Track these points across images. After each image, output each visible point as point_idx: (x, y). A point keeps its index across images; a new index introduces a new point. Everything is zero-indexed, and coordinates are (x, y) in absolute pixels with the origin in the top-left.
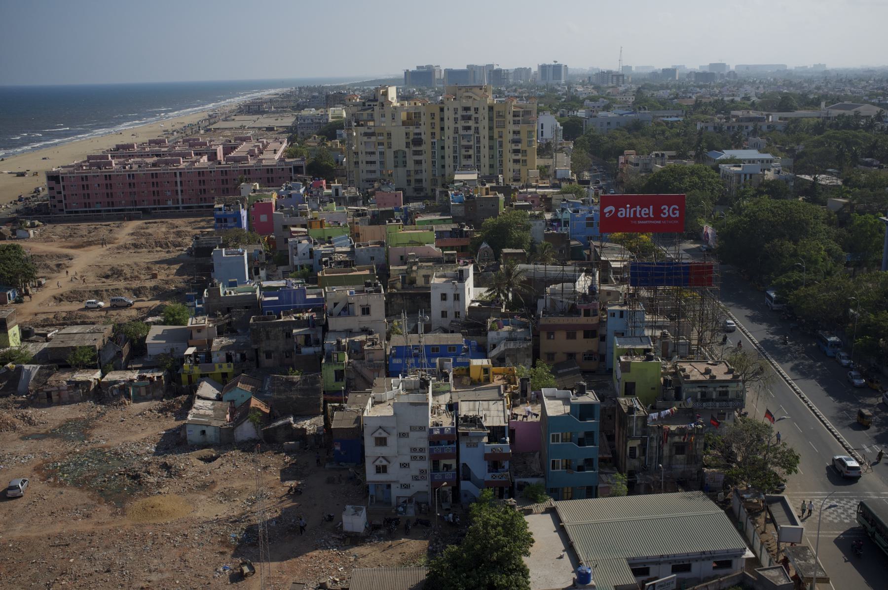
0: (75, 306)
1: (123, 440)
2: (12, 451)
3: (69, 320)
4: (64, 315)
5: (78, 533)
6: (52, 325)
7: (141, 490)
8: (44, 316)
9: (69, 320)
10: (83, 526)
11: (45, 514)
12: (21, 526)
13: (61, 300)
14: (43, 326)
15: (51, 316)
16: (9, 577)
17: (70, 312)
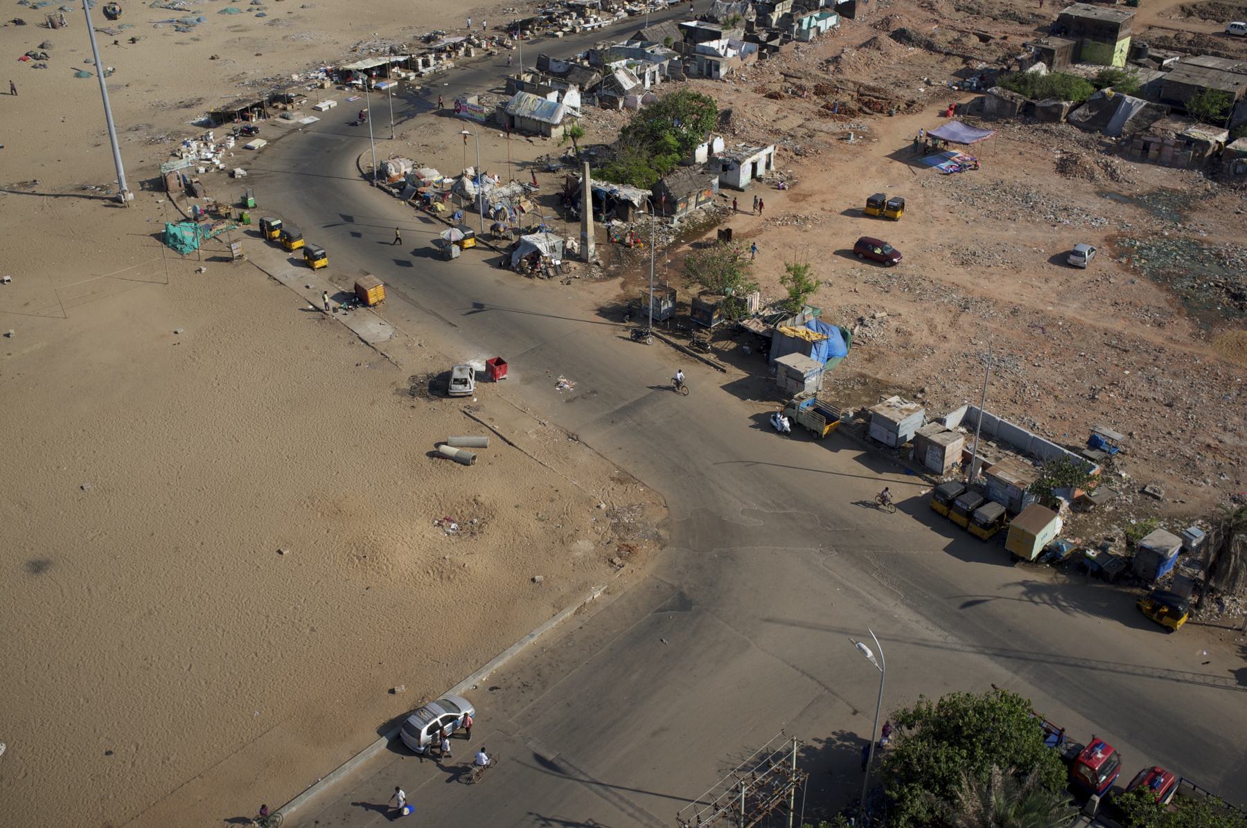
0: (1209, 28)
1: (1234, 240)
2: (1084, 206)
3: (1196, 46)
4: (1190, 37)
5: (1143, 341)
6: (1170, 49)
7: (1241, 317)
8: (1161, 33)
9: (1196, 46)
10: (1148, 333)
11: (1107, 301)
12: (1076, 305)
13: (1190, 14)
14: (1157, 47)
15: (1171, 35)
16: (1053, 361)
17: (1199, 35)
